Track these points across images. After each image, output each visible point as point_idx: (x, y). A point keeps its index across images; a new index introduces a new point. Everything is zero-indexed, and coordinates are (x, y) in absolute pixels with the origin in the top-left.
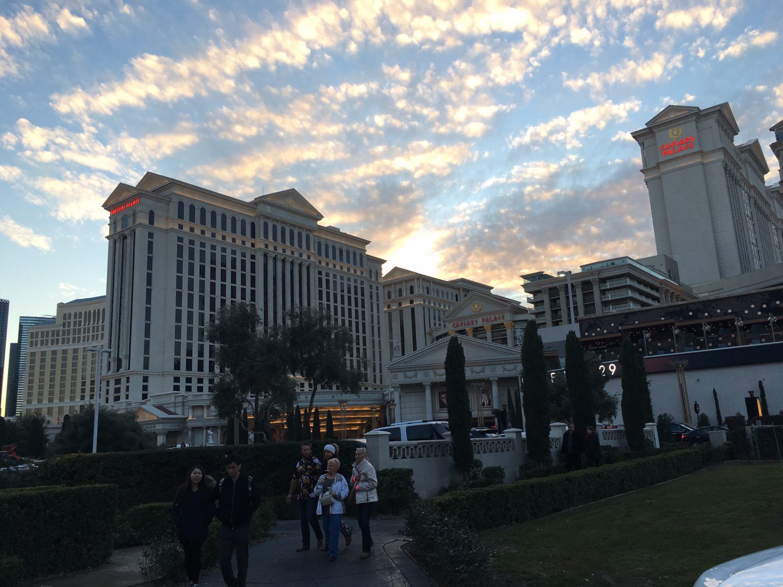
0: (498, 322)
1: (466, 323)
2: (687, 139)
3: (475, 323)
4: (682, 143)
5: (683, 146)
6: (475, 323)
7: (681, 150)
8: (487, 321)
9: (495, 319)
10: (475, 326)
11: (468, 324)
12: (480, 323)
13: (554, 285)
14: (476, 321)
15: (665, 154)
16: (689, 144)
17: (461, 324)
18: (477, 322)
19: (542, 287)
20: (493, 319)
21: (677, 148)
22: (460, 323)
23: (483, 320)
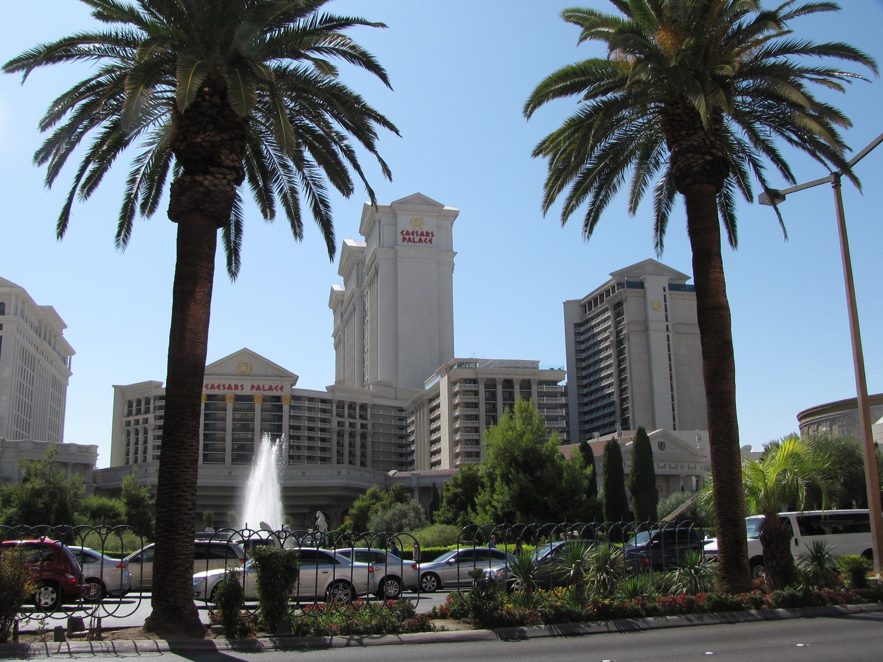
0: (274, 393)
1: (227, 386)
2: (427, 234)
3: (240, 388)
4: (422, 234)
5: (423, 238)
6: (240, 388)
7: (420, 241)
8: (258, 388)
9: (271, 388)
10: (239, 392)
11: (230, 387)
12: (247, 391)
13: (493, 377)
14: (242, 386)
15: (404, 239)
16: (429, 238)
17: (219, 387)
18: (243, 389)
19: (480, 376)
20: (267, 387)
21: (417, 239)
22: (216, 385)
23: (253, 387)
